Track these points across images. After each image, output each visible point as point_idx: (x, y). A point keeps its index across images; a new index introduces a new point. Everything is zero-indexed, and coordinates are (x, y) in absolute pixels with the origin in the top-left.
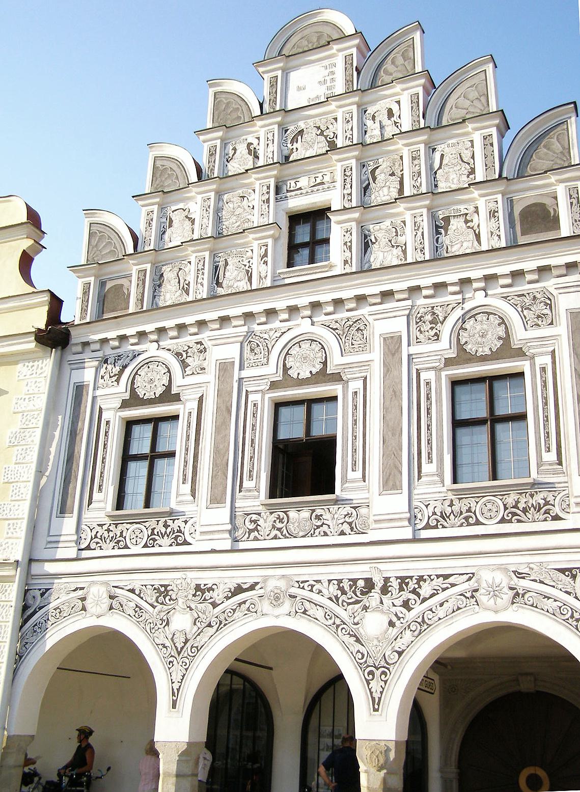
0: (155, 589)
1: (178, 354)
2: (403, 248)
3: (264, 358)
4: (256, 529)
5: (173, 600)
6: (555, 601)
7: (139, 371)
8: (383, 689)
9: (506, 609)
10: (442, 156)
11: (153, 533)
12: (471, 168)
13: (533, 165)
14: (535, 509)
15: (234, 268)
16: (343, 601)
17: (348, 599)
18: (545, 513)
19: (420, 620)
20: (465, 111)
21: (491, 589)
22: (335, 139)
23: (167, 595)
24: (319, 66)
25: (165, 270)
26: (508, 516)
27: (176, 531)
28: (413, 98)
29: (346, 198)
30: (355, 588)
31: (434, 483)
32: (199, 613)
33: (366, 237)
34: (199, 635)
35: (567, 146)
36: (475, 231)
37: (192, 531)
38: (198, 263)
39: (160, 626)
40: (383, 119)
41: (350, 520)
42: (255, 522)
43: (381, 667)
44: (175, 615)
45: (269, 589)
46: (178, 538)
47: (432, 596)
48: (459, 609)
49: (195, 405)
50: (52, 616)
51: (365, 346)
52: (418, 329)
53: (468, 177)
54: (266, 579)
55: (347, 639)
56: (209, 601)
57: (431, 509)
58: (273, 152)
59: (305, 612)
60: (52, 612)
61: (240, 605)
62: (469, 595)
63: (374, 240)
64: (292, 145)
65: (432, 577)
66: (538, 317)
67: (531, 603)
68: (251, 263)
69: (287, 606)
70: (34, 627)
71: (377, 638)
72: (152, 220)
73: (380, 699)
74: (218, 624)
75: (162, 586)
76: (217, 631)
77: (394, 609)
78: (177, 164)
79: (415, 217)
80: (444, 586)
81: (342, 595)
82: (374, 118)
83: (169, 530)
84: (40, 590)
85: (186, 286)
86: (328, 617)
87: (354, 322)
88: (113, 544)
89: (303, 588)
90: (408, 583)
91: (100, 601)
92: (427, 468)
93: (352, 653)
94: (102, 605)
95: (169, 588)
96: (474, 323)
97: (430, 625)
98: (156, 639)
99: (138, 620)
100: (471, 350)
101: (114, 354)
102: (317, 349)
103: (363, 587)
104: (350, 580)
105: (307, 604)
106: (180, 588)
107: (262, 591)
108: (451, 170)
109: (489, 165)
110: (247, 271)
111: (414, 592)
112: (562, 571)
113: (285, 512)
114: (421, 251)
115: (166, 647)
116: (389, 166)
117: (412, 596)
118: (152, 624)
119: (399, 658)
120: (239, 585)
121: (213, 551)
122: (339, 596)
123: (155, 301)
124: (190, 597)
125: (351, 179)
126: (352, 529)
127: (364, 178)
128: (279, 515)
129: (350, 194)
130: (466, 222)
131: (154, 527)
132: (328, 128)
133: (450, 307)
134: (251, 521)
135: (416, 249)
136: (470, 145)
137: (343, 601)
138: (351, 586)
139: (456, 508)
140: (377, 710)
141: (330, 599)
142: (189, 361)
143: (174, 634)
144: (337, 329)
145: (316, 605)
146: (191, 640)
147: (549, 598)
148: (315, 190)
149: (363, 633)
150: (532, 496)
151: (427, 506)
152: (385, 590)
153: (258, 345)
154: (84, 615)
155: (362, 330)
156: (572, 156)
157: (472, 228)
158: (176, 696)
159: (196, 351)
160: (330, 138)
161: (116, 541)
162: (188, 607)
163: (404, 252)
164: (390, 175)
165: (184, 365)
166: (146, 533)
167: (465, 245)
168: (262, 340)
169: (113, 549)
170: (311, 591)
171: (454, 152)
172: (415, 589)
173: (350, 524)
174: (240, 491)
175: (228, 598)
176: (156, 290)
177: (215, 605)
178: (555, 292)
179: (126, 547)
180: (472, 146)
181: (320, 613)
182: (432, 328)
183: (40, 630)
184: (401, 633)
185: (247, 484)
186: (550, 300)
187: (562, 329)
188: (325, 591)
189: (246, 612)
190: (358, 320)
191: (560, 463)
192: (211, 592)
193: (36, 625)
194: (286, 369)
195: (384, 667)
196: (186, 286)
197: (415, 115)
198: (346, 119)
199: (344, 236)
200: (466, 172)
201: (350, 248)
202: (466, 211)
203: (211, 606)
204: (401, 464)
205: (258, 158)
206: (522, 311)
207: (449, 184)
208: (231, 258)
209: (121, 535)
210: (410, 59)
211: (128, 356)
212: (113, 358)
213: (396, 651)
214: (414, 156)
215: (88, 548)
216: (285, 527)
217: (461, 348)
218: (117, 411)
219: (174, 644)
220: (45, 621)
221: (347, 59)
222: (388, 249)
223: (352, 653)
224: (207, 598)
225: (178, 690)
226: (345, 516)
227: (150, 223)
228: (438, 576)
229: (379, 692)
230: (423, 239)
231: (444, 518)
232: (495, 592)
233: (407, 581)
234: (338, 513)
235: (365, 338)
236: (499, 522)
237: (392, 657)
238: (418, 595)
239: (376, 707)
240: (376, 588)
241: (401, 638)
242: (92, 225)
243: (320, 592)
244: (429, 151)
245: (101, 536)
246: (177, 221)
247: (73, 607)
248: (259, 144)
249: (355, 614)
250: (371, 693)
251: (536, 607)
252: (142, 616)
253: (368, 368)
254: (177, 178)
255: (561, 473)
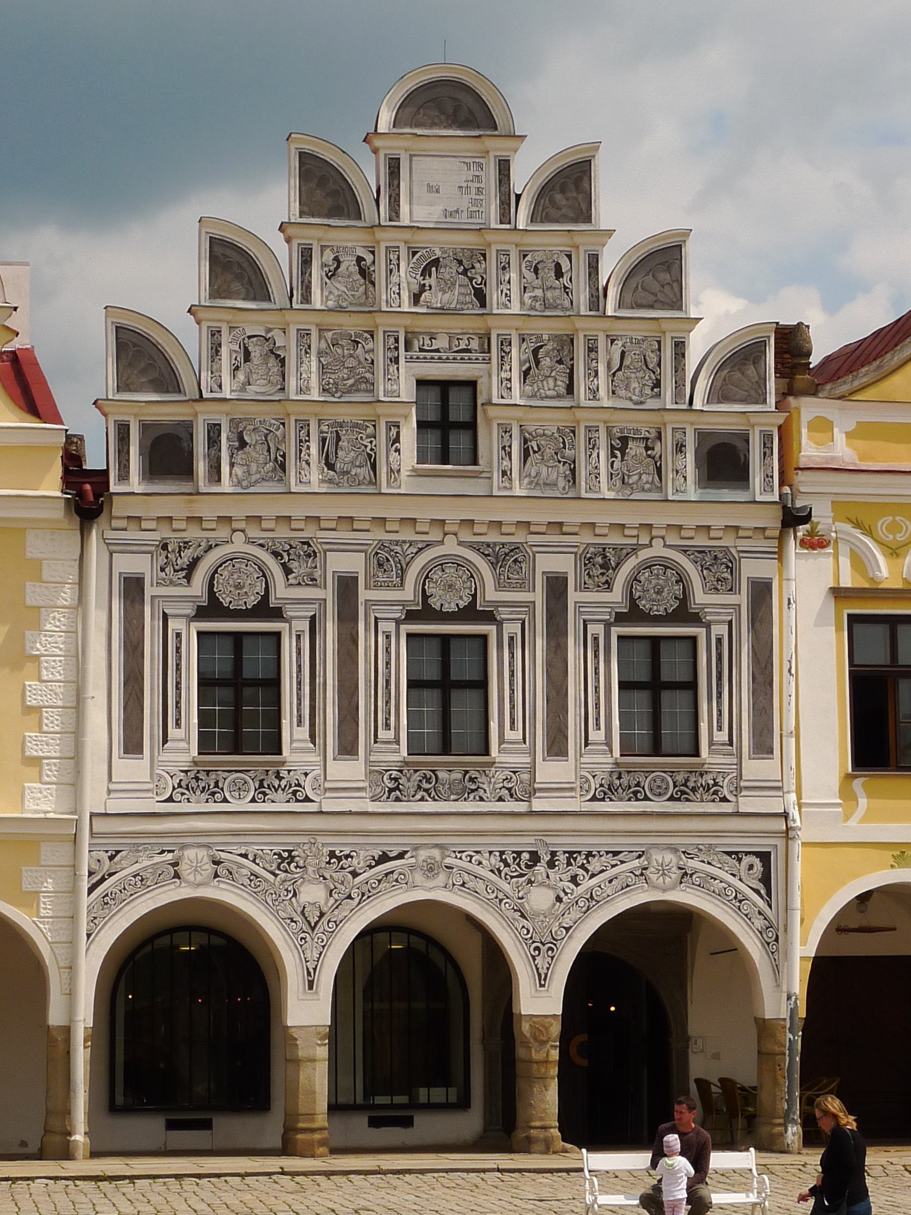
0: (275, 854)
1: (276, 554)
2: (572, 466)
3: (397, 577)
4: (397, 788)
5: (301, 868)
6: (721, 882)
7: (219, 569)
8: (550, 965)
9: (673, 888)
10: (623, 354)
11: (261, 786)
12: (657, 379)
13: (724, 392)
14: (704, 789)
15: (350, 448)
16: (506, 874)
17: (512, 872)
18: (713, 794)
19: (588, 896)
20: (652, 298)
21: (660, 868)
22: (483, 286)
23: (292, 861)
24: (458, 160)
25: (245, 428)
26: (677, 794)
27: (293, 785)
28: (591, 259)
29: (504, 384)
30: (520, 861)
31: (604, 753)
32: (336, 884)
33: (526, 441)
34: (337, 907)
35: (763, 377)
36: (656, 463)
37: (316, 785)
38: (300, 431)
39: (284, 898)
40: (549, 275)
41: (510, 785)
42: (396, 779)
43: (547, 943)
44: (304, 885)
45: (421, 858)
46: (296, 794)
47: (602, 871)
48: (628, 886)
49: (305, 626)
50: (130, 885)
51: (525, 585)
52: (587, 572)
53: (652, 390)
54: (416, 848)
55: (510, 913)
56: (348, 870)
57: (598, 781)
58: (399, 285)
59: (463, 885)
60: (130, 880)
61: (386, 875)
62: (637, 873)
63: (536, 449)
64: (424, 279)
65: (601, 853)
66: (718, 580)
67: (698, 883)
68: (374, 443)
69: (441, 878)
70: (104, 897)
71: (543, 914)
72: (220, 345)
73: (546, 975)
74: (360, 897)
75: (284, 851)
76: (359, 903)
77: (561, 884)
78: (248, 261)
79: (589, 431)
80: (614, 863)
81: (505, 867)
82: (536, 271)
83: (283, 783)
84: (107, 851)
85: (280, 458)
86: (490, 891)
87: (512, 551)
88: (205, 796)
89: (461, 858)
90: (576, 858)
91: (200, 867)
92: (594, 736)
93: (516, 929)
94: (203, 872)
95: (293, 854)
96: (649, 576)
97: (598, 902)
98: (280, 912)
99: (255, 890)
100: (644, 606)
101: (176, 538)
102: (464, 577)
103: (528, 860)
104: (514, 852)
105: (466, 877)
106: (309, 854)
107: (413, 860)
108: (633, 375)
109: (679, 382)
110: (370, 456)
111: (582, 867)
112: (729, 854)
113: (433, 771)
114: (596, 477)
115: (295, 922)
116: (556, 349)
117: (581, 872)
118: (274, 896)
119: (567, 933)
120: (383, 852)
121: (350, 813)
122: (501, 869)
123: (233, 472)
124: (323, 865)
125: (511, 358)
126: (511, 796)
127: (524, 357)
128: (425, 774)
129: (510, 380)
130: (647, 448)
131: (262, 777)
132: (473, 267)
133: (625, 551)
134: (391, 779)
135: (590, 474)
136: (657, 347)
137: (506, 874)
138: (514, 859)
139: (625, 780)
140: (544, 986)
141: (492, 871)
142: (294, 565)
143: (304, 907)
144: (489, 555)
145: (476, 877)
146: (326, 916)
147: (715, 879)
148: (459, 358)
149: (528, 908)
150: (701, 775)
151: (594, 777)
152: (551, 864)
153: (388, 560)
154: (177, 884)
155: (520, 562)
156: (768, 391)
157: (653, 458)
158: (312, 974)
159: (302, 553)
160: (476, 283)
161: (209, 792)
162: (320, 876)
163: (573, 471)
164: (557, 362)
165: (287, 571)
166: (252, 785)
167: (644, 477)
168: (392, 553)
169: (207, 802)
170: (470, 861)
171: (637, 352)
172: (583, 864)
173: (509, 789)
174: (376, 742)
175: (371, 867)
176: (233, 454)
177: (355, 874)
178: (737, 558)
179: (225, 800)
180: (659, 350)
181: (481, 886)
182: (603, 574)
183: (114, 902)
184: (569, 909)
185: (383, 734)
186: (732, 563)
187: (742, 599)
188: (484, 862)
189: (395, 883)
190: (515, 549)
191: (731, 744)
192: (350, 859)
193: (107, 895)
194: (425, 597)
195: (552, 943)
196: (280, 458)
197: (592, 286)
198: (501, 263)
199: (502, 437)
200: (650, 383)
201: (510, 455)
202: (647, 435)
203: (350, 876)
204: (567, 728)
205: (373, 284)
206: (702, 571)
207: (629, 395)
208: (344, 432)
209: (216, 785)
210: (586, 192)
211: (200, 546)
212: (176, 544)
213: (564, 928)
214: (590, 345)
215: (170, 800)
216: (433, 789)
217: (633, 603)
218: (191, 621)
219: (306, 918)
220: (121, 891)
221: (502, 166)
222: (551, 463)
223: (516, 929)
224: (344, 866)
225: (315, 969)
226: (504, 780)
227: (217, 352)
228: (607, 853)
229: (545, 968)
230: (599, 462)
231: (612, 792)
232: (663, 871)
233: (575, 856)
234: (496, 776)
235: (524, 572)
236: (668, 800)
237: (559, 933)
238: (587, 871)
239: (543, 982)
240: (542, 861)
241: (569, 914)
242: (120, 330)
243: (480, 863)
244: (607, 341)
245: (187, 785)
246: (257, 354)
247: (160, 875)
248: (374, 262)
249: (520, 889)
250: (537, 969)
251: (703, 887)
252: (259, 886)
253: (527, 609)
254: (250, 281)
255: (730, 755)
